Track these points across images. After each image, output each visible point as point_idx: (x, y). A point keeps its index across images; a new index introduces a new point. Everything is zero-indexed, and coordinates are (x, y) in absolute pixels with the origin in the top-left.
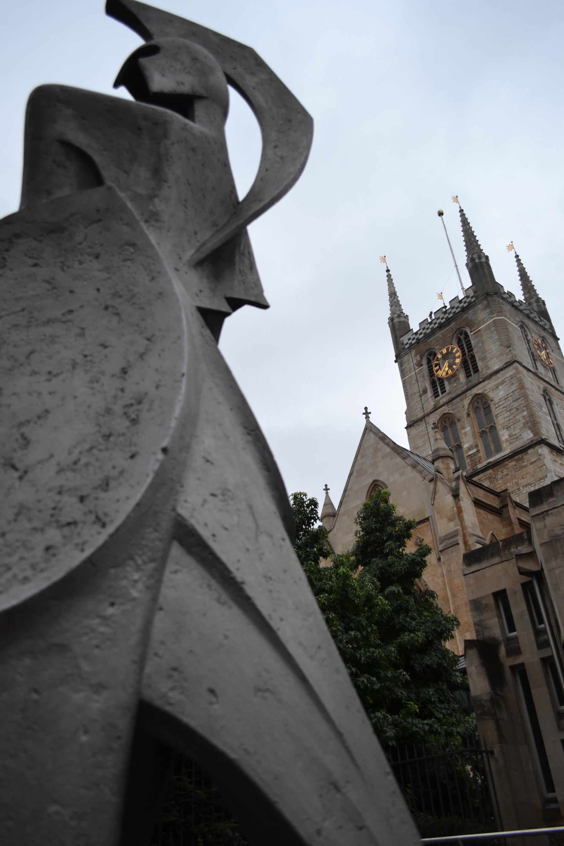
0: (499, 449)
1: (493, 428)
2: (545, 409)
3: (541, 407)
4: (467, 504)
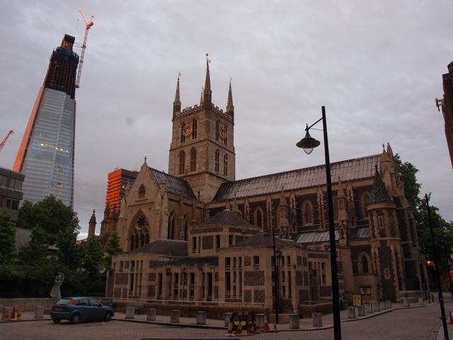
0: (195, 170)
1: (195, 162)
2: (214, 158)
3: (212, 157)
4: (166, 201)
